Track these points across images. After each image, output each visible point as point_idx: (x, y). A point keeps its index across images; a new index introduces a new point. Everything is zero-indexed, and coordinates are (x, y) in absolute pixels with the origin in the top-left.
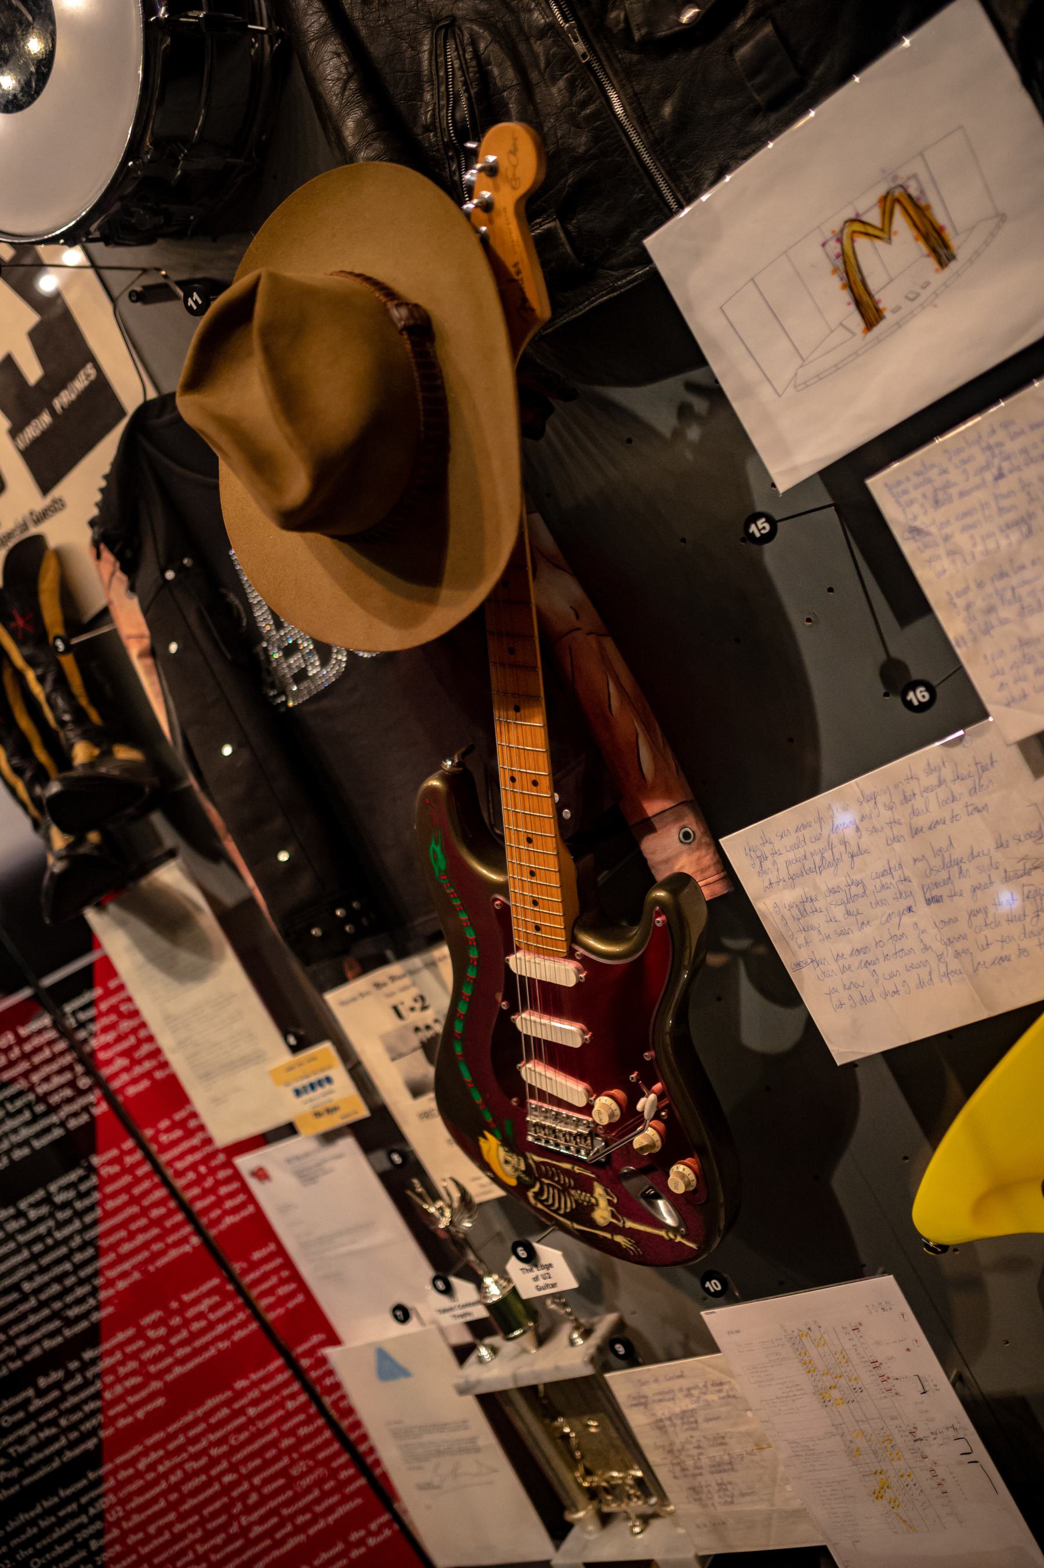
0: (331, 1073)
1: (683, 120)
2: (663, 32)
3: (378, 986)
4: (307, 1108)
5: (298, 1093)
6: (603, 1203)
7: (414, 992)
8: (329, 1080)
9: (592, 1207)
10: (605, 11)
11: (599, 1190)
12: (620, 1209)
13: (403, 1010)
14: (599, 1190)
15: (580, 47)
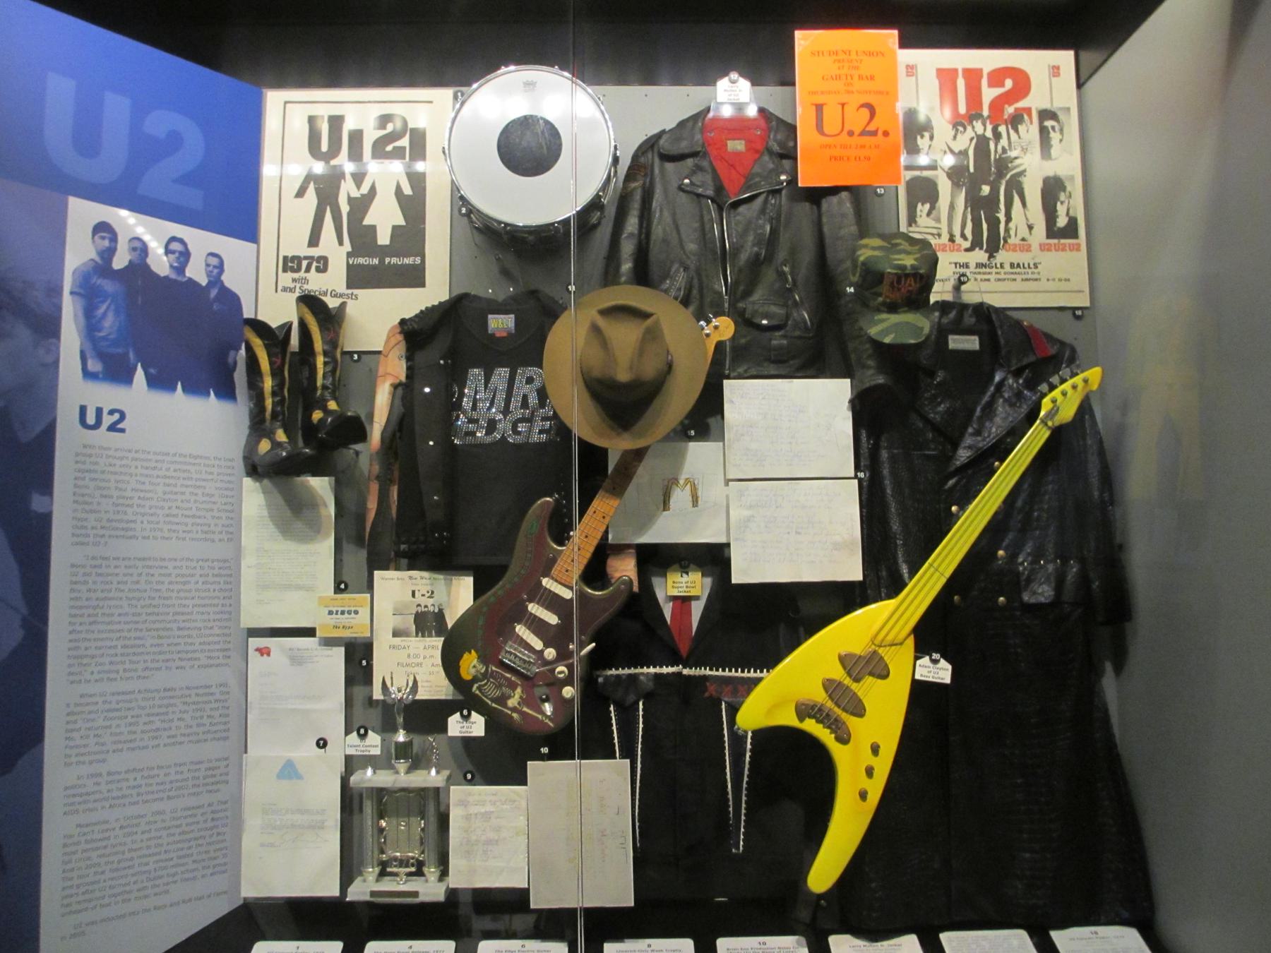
0: (359, 609)
1: (746, 348)
2: (756, 320)
3: (411, 578)
4: (332, 622)
5: (330, 613)
6: (517, 696)
7: (429, 588)
8: (356, 612)
9: (509, 697)
10: (738, 301)
11: (519, 690)
12: (523, 701)
13: (417, 594)
14: (519, 690)
15: (726, 305)
